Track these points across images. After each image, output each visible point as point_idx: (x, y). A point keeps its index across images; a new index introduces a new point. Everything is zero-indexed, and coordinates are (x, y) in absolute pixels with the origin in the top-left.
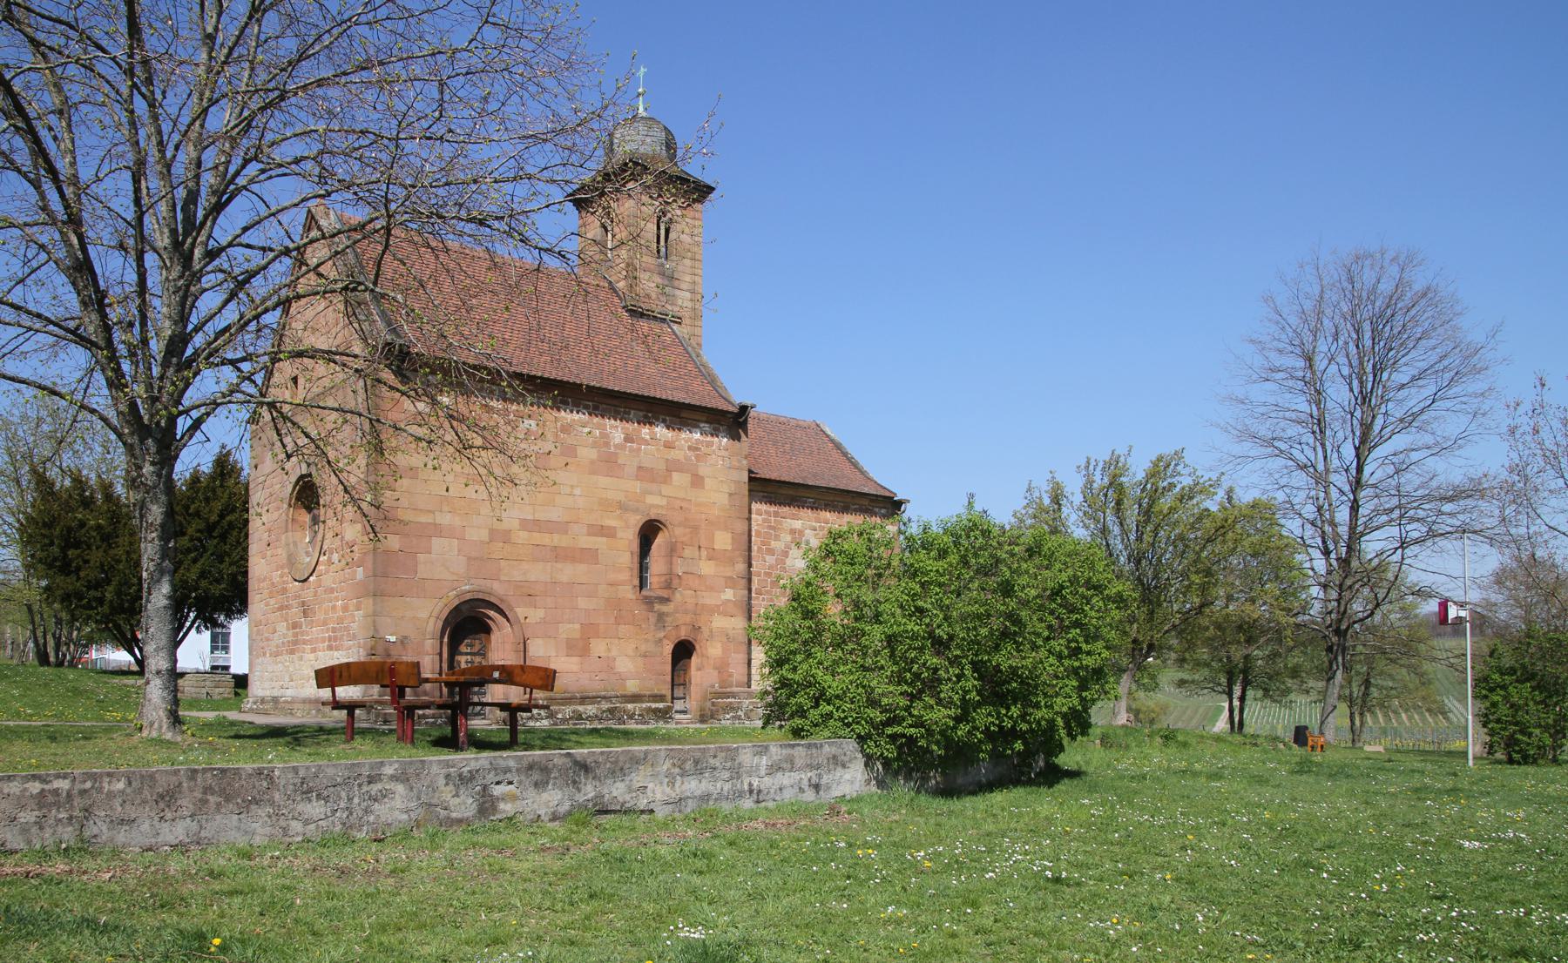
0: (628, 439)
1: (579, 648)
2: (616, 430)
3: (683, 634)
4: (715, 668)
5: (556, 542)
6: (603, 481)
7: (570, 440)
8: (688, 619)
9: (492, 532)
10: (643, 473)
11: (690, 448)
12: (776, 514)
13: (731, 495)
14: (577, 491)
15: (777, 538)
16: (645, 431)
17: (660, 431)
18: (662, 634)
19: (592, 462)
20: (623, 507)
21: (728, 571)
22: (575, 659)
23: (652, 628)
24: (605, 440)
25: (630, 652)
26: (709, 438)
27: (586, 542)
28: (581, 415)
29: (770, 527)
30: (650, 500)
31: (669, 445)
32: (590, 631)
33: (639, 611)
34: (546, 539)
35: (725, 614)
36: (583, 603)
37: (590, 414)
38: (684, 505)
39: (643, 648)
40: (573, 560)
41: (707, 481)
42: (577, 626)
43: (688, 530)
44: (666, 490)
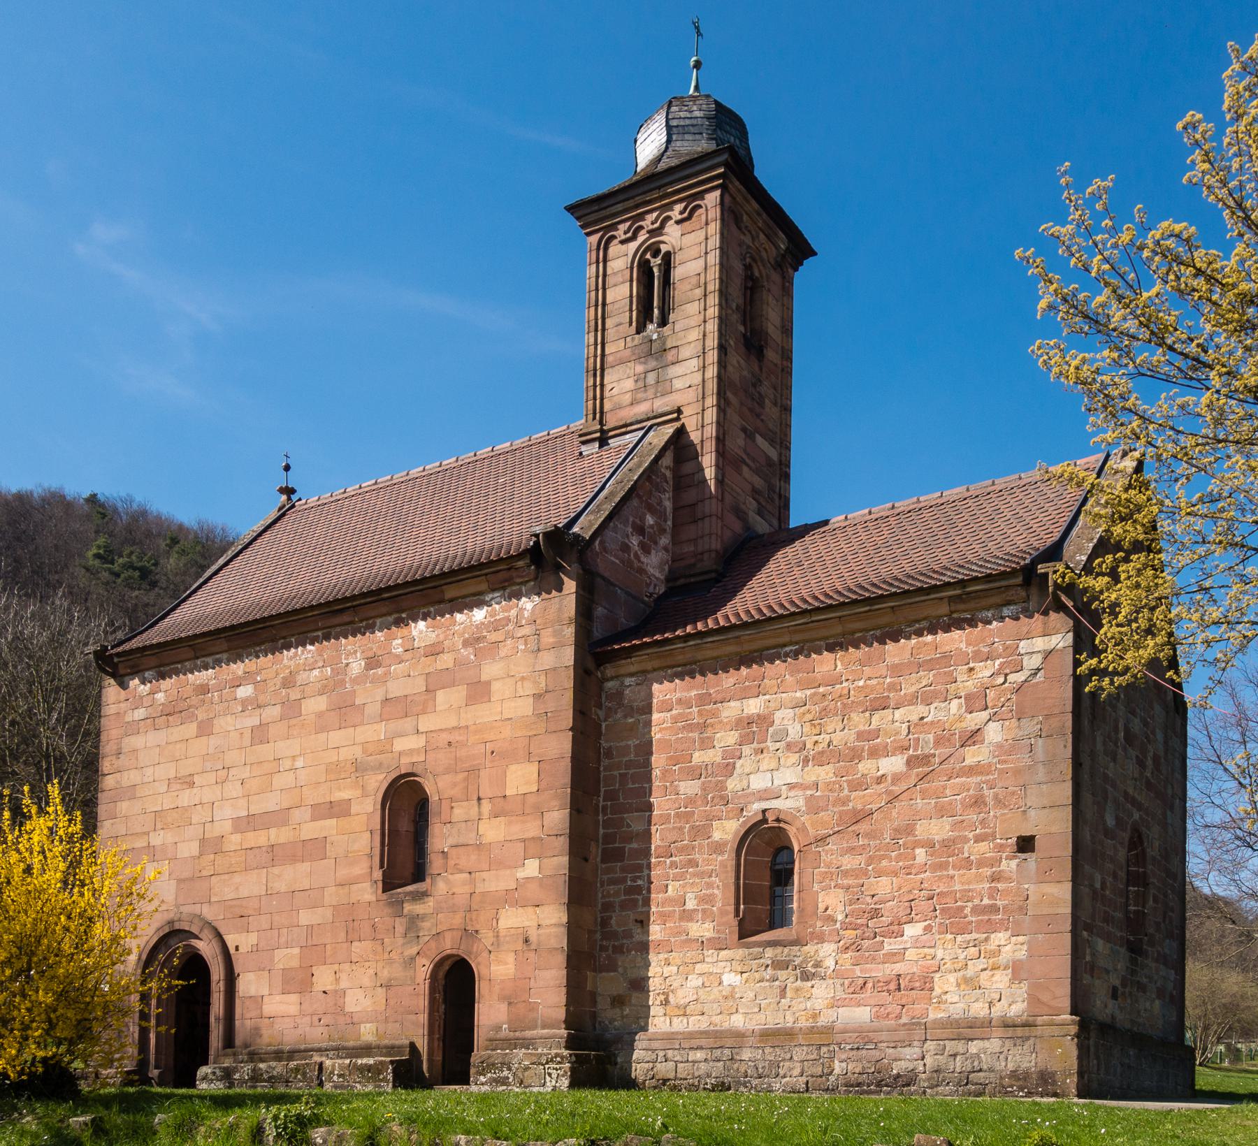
0: (372, 662)
1: (299, 981)
3: (449, 945)
4: (502, 998)
6: (336, 737)
8: (457, 920)
9: (203, 841)
11: (466, 643)
12: (703, 700)
13: (538, 697)
14: (299, 763)
15: (707, 744)
19: (320, 715)
20: (359, 768)
21: (531, 829)
22: (294, 998)
23: (400, 941)
25: (366, 981)
27: (311, 830)
29: (690, 728)
30: (400, 745)
31: (434, 651)
32: (314, 953)
33: (382, 916)
34: (260, 838)
37: (273, 654)
38: (455, 737)
39: (385, 974)
40: (294, 859)
41: (496, 686)
42: (296, 951)
43: (461, 776)
44: (426, 723)
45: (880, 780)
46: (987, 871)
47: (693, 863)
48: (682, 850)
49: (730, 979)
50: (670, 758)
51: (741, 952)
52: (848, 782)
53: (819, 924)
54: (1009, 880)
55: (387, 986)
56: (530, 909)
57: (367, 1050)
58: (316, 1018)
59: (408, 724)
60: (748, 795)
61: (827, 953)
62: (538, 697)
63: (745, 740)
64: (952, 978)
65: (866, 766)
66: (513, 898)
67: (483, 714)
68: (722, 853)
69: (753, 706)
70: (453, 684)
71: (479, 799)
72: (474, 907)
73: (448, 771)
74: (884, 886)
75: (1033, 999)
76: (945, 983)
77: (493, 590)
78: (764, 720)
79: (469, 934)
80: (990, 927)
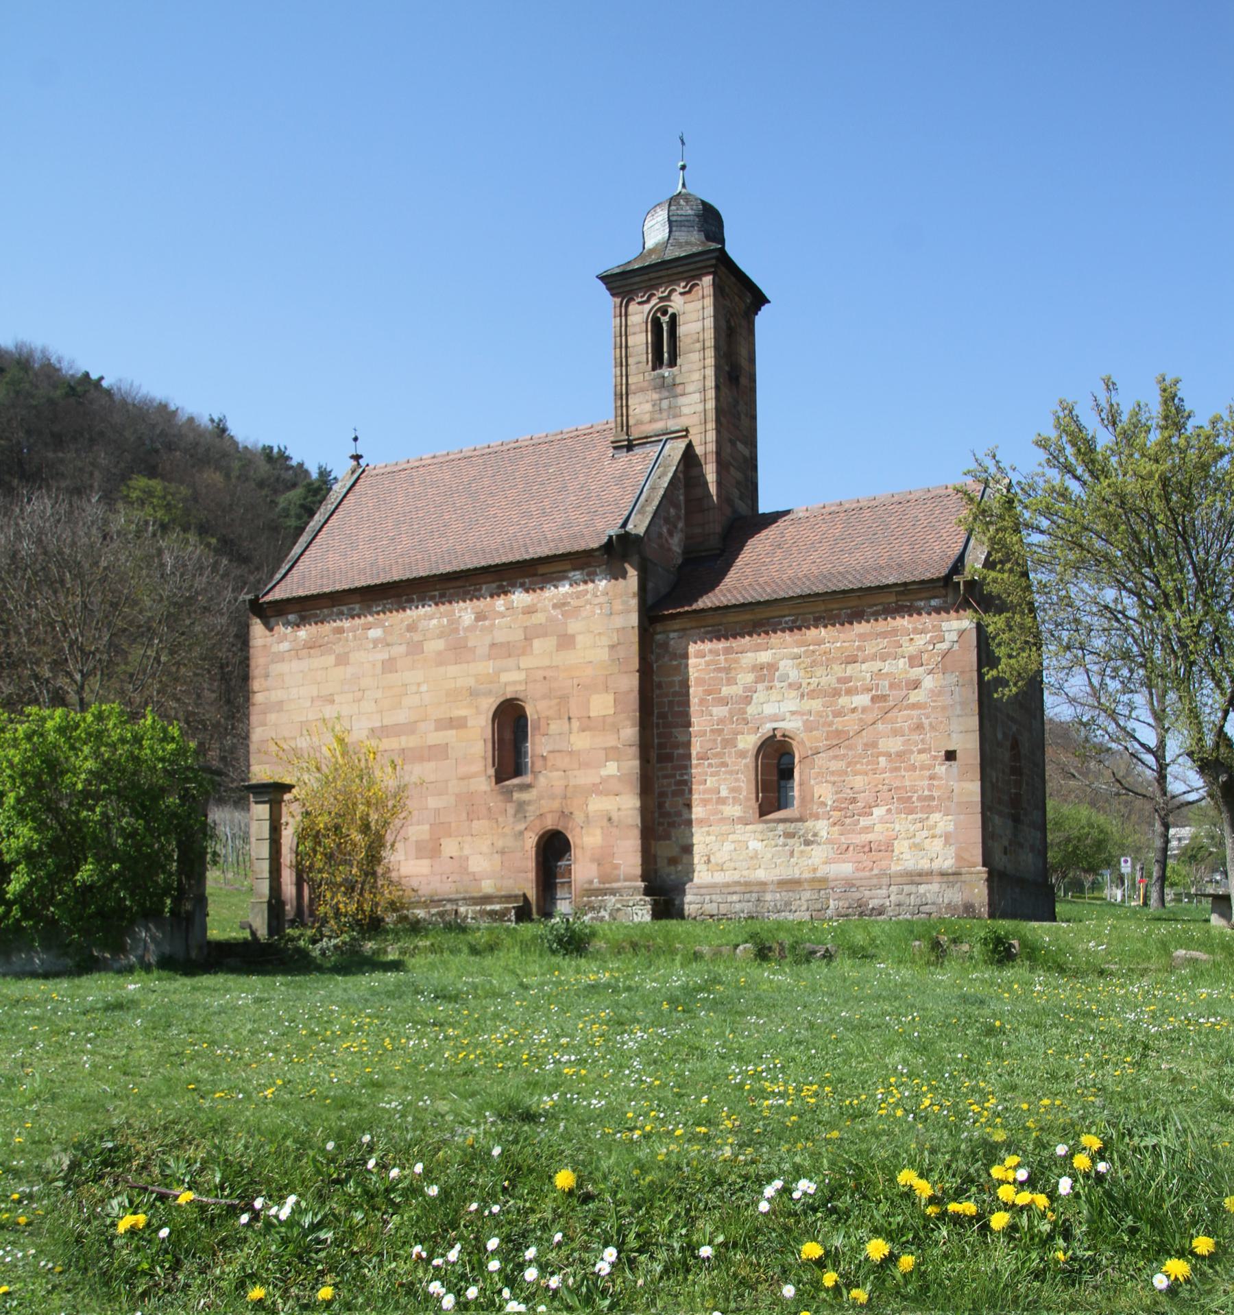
0: (480, 617)
1: (430, 849)
2: (465, 612)
3: (550, 823)
4: (593, 860)
5: (404, 745)
6: (452, 670)
7: (417, 637)
8: (556, 805)
10: (502, 650)
11: (555, 606)
13: (612, 647)
14: (424, 688)
15: (731, 681)
16: (500, 603)
17: (519, 598)
18: (522, 826)
19: (439, 653)
20: (473, 693)
22: (426, 862)
23: (511, 820)
24: (454, 624)
25: (485, 849)
26: (582, 587)
27: (435, 738)
28: (427, 608)
30: (505, 677)
31: (530, 611)
33: (496, 802)
35: (606, 793)
36: (433, 802)
38: (549, 674)
39: (500, 844)
41: (579, 638)
42: (427, 827)
43: (554, 702)
44: (525, 662)
45: (854, 710)
46: (927, 773)
47: (724, 764)
48: (717, 755)
49: (754, 845)
50: (705, 691)
51: (761, 827)
52: (833, 712)
53: (815, 807)
54: (941, 779)
55: (502, 852)
56: (612, 798)
57: (487, 899)
58: (444, 877)
59: (511, 662)
60: (763, 719)
61: (822, 827)
62: (612, 647)
63: (759, 680)
64: (906, 843)
65: (843, 701)
66: (598, 789)
67: (569, 658)
68: (745, 757)
69: (764, 657)
70: (545, 635)
71: (569, 718)
72: (569, 795)
73: (544, 697)
74: (859, 782)
75: (959, 858)
76: (901, 846)
77: (574, 569)
78: (773, 667)
79: (565, 815)
80: (929, 810)
